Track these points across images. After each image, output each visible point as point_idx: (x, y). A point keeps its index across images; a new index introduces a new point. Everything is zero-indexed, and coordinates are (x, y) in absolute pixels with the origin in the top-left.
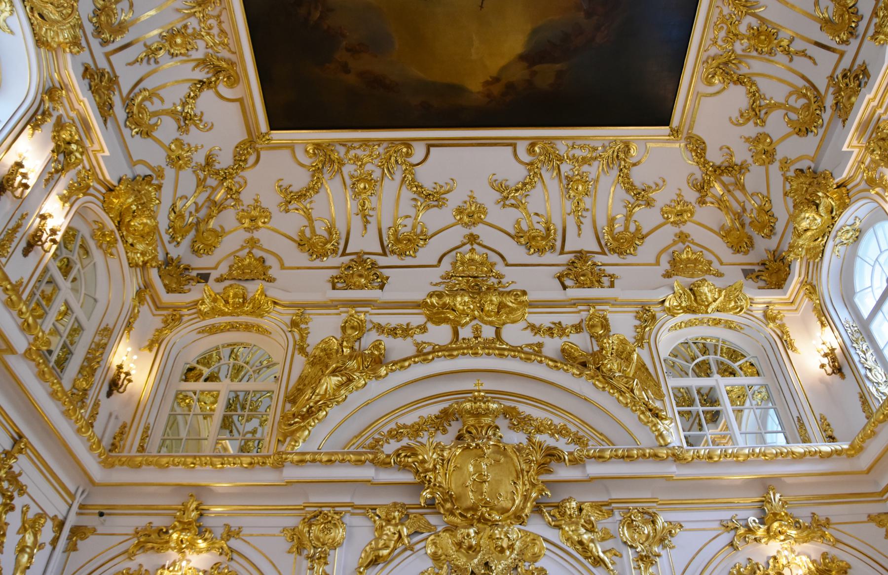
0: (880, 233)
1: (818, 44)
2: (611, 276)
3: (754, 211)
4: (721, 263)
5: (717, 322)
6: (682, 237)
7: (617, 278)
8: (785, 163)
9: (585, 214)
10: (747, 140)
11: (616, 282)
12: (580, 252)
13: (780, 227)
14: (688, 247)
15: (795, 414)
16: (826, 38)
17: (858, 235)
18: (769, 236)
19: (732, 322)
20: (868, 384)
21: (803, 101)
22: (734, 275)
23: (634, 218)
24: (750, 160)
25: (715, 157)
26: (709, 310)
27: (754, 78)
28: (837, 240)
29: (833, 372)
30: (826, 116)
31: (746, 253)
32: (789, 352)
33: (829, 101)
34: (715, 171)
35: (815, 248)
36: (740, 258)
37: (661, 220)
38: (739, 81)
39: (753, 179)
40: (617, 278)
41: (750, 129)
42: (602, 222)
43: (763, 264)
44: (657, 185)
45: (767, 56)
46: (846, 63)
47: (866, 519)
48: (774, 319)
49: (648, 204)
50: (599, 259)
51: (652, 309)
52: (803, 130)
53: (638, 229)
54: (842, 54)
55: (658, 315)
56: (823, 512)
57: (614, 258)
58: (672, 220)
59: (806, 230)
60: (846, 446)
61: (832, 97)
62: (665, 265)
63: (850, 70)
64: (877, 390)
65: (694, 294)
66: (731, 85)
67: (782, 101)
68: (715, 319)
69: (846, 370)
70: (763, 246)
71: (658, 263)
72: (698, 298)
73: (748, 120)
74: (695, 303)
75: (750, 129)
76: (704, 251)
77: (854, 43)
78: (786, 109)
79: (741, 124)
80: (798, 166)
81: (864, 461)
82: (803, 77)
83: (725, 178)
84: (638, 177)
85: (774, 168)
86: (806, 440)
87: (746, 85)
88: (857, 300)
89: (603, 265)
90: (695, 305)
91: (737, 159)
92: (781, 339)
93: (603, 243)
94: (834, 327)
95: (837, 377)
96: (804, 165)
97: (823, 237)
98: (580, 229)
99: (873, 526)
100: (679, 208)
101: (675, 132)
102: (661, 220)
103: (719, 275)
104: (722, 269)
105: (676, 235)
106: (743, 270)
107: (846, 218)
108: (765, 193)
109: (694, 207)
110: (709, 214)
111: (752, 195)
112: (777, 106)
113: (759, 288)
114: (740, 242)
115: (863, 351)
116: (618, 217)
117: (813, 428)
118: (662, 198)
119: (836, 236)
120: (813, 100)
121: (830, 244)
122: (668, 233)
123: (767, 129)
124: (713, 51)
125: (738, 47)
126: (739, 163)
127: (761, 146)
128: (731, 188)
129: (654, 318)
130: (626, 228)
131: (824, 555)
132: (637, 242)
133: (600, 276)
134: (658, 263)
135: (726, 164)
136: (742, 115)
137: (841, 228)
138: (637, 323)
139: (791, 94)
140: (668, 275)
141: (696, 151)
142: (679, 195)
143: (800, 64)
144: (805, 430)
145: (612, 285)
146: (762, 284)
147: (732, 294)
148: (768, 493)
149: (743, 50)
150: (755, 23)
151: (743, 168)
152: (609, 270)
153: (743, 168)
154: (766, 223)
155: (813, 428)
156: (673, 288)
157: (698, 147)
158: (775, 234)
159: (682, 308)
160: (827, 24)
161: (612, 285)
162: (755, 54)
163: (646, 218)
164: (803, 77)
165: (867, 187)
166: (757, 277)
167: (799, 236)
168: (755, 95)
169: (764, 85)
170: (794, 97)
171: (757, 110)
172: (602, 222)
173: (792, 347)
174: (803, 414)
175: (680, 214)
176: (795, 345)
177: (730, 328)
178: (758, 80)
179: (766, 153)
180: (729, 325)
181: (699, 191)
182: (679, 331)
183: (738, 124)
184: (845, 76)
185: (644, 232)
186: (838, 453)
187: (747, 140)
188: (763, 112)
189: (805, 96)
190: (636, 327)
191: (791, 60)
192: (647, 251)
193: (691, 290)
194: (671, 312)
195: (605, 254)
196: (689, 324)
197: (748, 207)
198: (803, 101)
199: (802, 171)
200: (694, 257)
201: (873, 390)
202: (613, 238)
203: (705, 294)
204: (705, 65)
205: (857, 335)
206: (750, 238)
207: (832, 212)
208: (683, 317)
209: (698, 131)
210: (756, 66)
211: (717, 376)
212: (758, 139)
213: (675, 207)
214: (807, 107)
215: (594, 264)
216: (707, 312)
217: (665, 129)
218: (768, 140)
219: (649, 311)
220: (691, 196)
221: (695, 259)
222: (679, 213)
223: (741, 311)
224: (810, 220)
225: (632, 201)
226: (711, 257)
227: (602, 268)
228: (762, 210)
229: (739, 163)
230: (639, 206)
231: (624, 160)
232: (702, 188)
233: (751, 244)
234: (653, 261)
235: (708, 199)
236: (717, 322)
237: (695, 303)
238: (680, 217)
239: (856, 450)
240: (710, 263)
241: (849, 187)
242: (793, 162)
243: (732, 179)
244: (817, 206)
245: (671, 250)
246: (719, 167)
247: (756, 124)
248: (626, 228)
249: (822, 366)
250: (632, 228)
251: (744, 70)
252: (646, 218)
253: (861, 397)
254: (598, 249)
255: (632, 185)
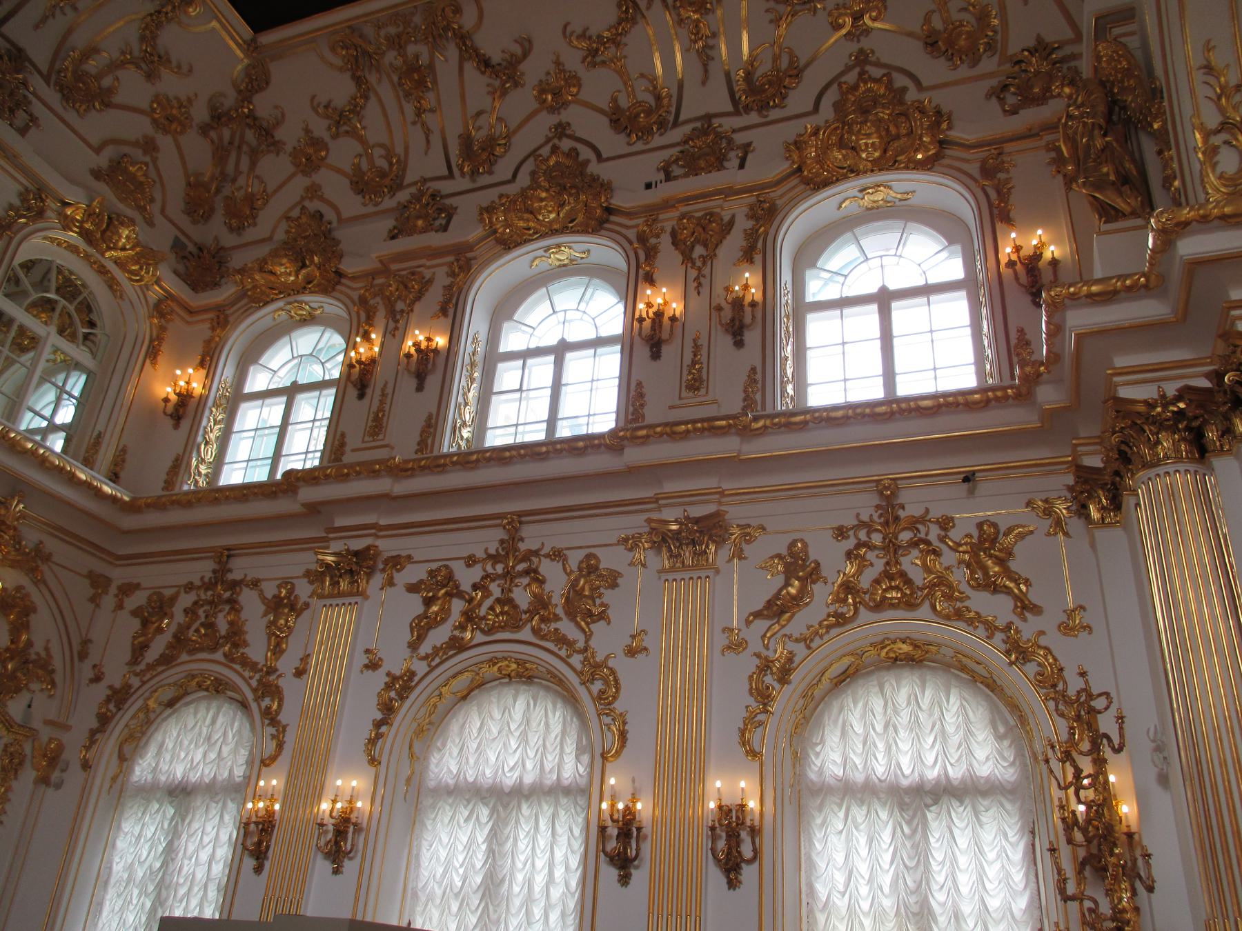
0: (327, 335)
1: (444, 140)
2: (33, 119)
3: (242, 192)
4: (163, 212)
5: (102, 271)
6: (149, 146)
7: (38, 126)
8: (313, 191)
9: (68, 10)
10: (307, 131)
11: (33, 131)
12: (20, 50)
13: (251, 234)
14: (146, 164)
15: (100, 427)
16: (454, 150)
17: (309, 320)
18: (231, 229)
19: (118, 284)
20: (194, 454)
21: (385, 165)
22: (161, 239)
23: (120, 73)
24: (289, 148)
25: (263, 105)
26: (107, 255)
27: (371, 95)
28: (289, 307)
29: (171, 416)
30: (389, 203)
31: (195, 222)
32: (148, 361)
33: (403, 196)
34: (248, 117)
35: (263, 293)
36: (185, 222)
37: (145, 105)
38: (358, 80)
39: (274, 167)
40: (38, 126)
41: (320, 128)
42: (80, 40)
43: (200, 249)
44: (179, 67)
45: (401, 94)
46: (446, 187)
47: (85, 572)
48: (162, 315)
49: (151, 76)
50: (37, 82)
51: (49, 202)
52: (361, 185)
53: (110, 91)
54: (451, 175)
55: (49, 213)
56: (51, 545)
57: (53, 97)
58: (156, 116)
59: (272, 273)
60: (126, 498)
61: (408, 197)
62: (103, 161)
63: (442, 197)
64: (197, 467)
65: (108, 225)
66: (349, 74)
67: (372, 142)
68: (104, 267)
69: (185, 424)
70: (216, 231)
71: (98, 151)
72: (109, 233)
73: (328, 117)
74: (99, 231)
75: (320, 128)
76: (158, 185)
77: (465, 184)
78: (367, 152)
79: (317, 112)
80: (324, 208)
81: (129, 522)
82: (407, 149)
83: (250, 135)
84: (170, 38)
85: (301, 182)
86: (88, 462)
87: (359, 91)
88: (252, 369)
89: (35, 94)
90: (99, 236)
91: (279, 134)
92: (151, 341)
93: (57, 66)
94: (210, 376)
95: (169, 422)
96: (330, 215)
97: (280, 293)
98: (44, 19)
99: (87, 582)
100: (174, 112)
101: (251, 47)
102: (145, 105)
103: (150, 223)
104: (159, 219)
105: (145, 137)
106: (176, 237)
107: (314, 300)
108: (269, 190)
109: (191, 126)
110: (198, 151)
111: (258, 177)
112: (362, 140)
113: (175, 272)
114: (198, 204)
115: (215, 420)
116: (105, 54)
117: (106, 455)
118: (170, 84)
119: (290, 303)
120: (392, 176)
121: (280, 304)
122: (140, 127)
123: (332, 144)
124: (369, 31)
125: (391, 57)
126: (277, 138)
127: (310, 151)
128: (245, 148)
129: (40, 214)
130: (99, 77)
131: (19, 588)
132: (97, 104)
133: (18, 105)
134: (98, 151)
135: (265, 124)
136: (326, 107)
137: (301, 302)
138: (17, 202)
139: (382, 146)
140: (97, 174)
141: (251, 81)
142: (190, 101)
143: (416, 135)
144: (97, 451)
145: (23, 131)
146: (181, 268)
147: (146, 256)
148: (13, 498)
149: (391, 64)
150: (424, 60)
151: (276, 146)
152: (38, 108)
153: (276, 146)
154: (243, 213)
155: (106, 455)
156: (92, 200)
157: (256, 80)
158: (239, 235)
159: (81, 227)
160: (466, 141)
161: (23, 131)
162: (395, 79)
163: (133, 87)
164: (407, 149)
165: (356, 298)
166: (184, 257)
167: (261, 270)
168: (356, 109)
169: (372, 110)
170: (382, 152)
171: (343, 119)
172: (80, 40)
173: (155, 358)
174: (108, 436)
175: (170, 119)
176: (159, 358)
177: (111, 287)
178: (373, 100)
179: (309, 158)
180: (112, 284)
181: (213, 117)
182: (54, 247)
183: (315, 110)
184: (433, 196)
185: (117, 99)
186: (114, 499)
187: (307, 131)
188: (346, 128)
189: (391, 164)
190: (11, 207)
191: (414, 123)
192: (99, 124)
193: (109, 218)
194: (67, 224)
195: (48, 84)
196: (73, 249)
197: (241, 181)
198: (385, 165)
199: (321, 216)
200: (142, 179)
201: (194, 462)
202: (74, 72)
203: (120, 237)
204: (347, 31)
205: (223, 401)
206: (212, 210)
207: (309, 283)
208: (73, 236)
209: (275, 68)
210: (386, 91)
211: (53, 329)
212: (317, 143)
213: (172, 107)
214: (383, 174)
215: (25, 84)
216: (103, 255)
217: (247, 32)
218: (323, 154)
219: (43, 201)
220: (200, 113)
221: (141, 183)
222: (170, 117)
223: (137, 281)
224: (285, 271)
225: (136, 53)
226: (158, 196)
227: (31, 97)
228: (250, 199)
229: (277, 138)
230: (139, 67)
231: (174, 7)
232: (218, 117)
233: (207, 217)
234: (95, 141)
235: (213, 134)
236: (102, 271)
237: (99, 231)
238: (166, 123)
239: (132, 507)
240: (152, 200)
241: (343, 281)
242: (322, 199)
243: (254, 142)
244: (304, 266)
245: (126, 149)
246: (255, 119)
247: (329, 128)
248: (99, 77)
249: (166, 400)
250: (107, 82)
251: (372, 78)
252: (133, 87)
253: (177, 460)
254: (44, 70)
255: (154, 38)
